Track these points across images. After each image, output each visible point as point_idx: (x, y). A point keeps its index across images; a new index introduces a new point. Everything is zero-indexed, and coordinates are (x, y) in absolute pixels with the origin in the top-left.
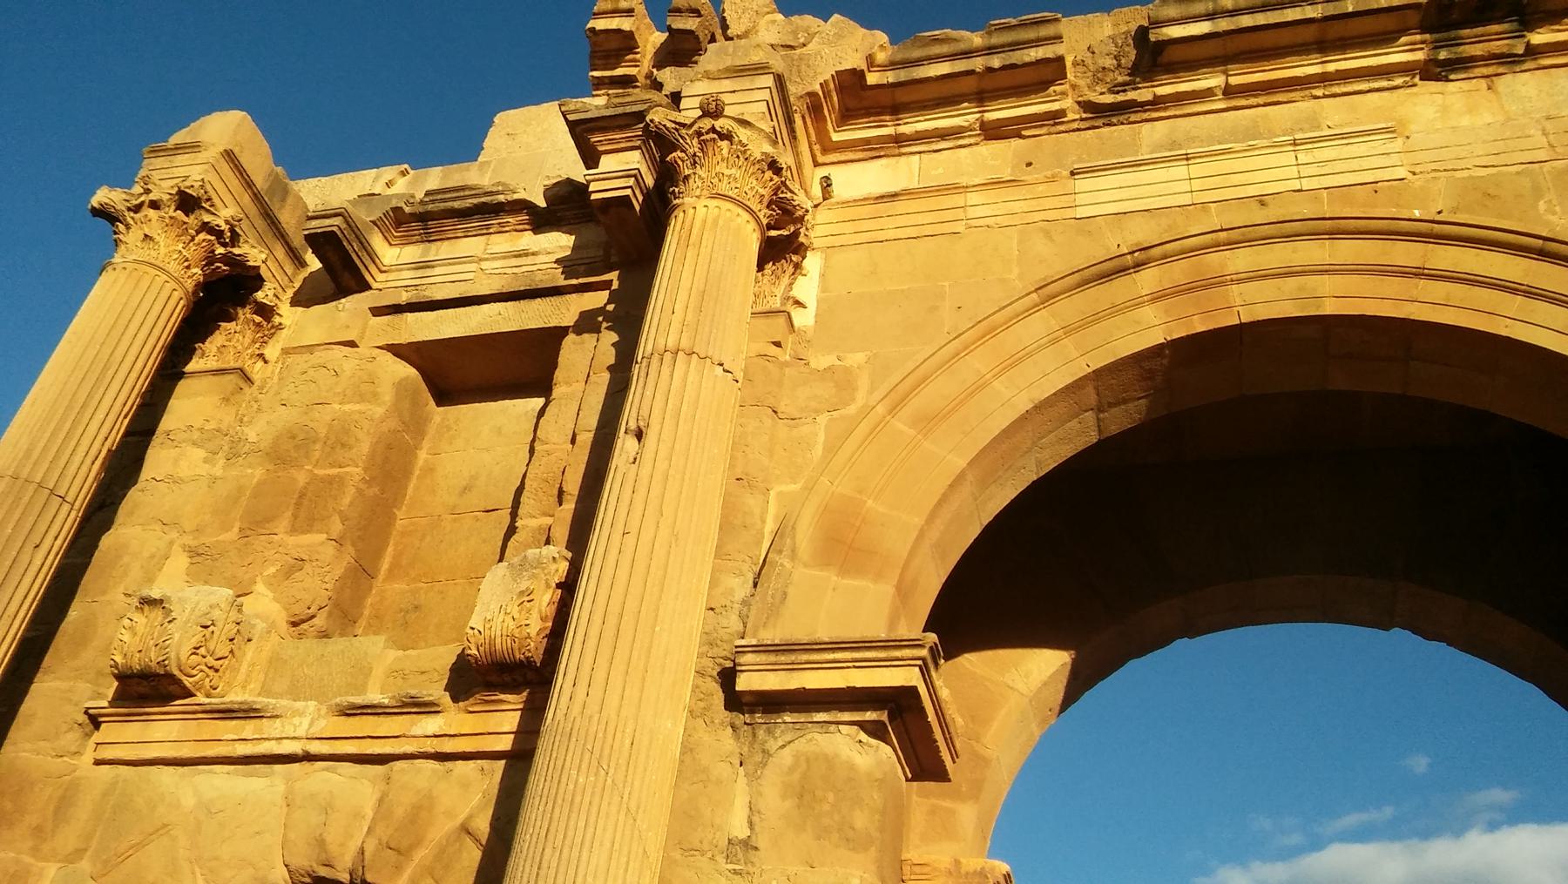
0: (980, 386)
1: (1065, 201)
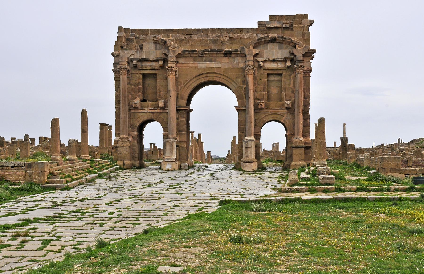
0: (191, 84)
1: (197, 66)
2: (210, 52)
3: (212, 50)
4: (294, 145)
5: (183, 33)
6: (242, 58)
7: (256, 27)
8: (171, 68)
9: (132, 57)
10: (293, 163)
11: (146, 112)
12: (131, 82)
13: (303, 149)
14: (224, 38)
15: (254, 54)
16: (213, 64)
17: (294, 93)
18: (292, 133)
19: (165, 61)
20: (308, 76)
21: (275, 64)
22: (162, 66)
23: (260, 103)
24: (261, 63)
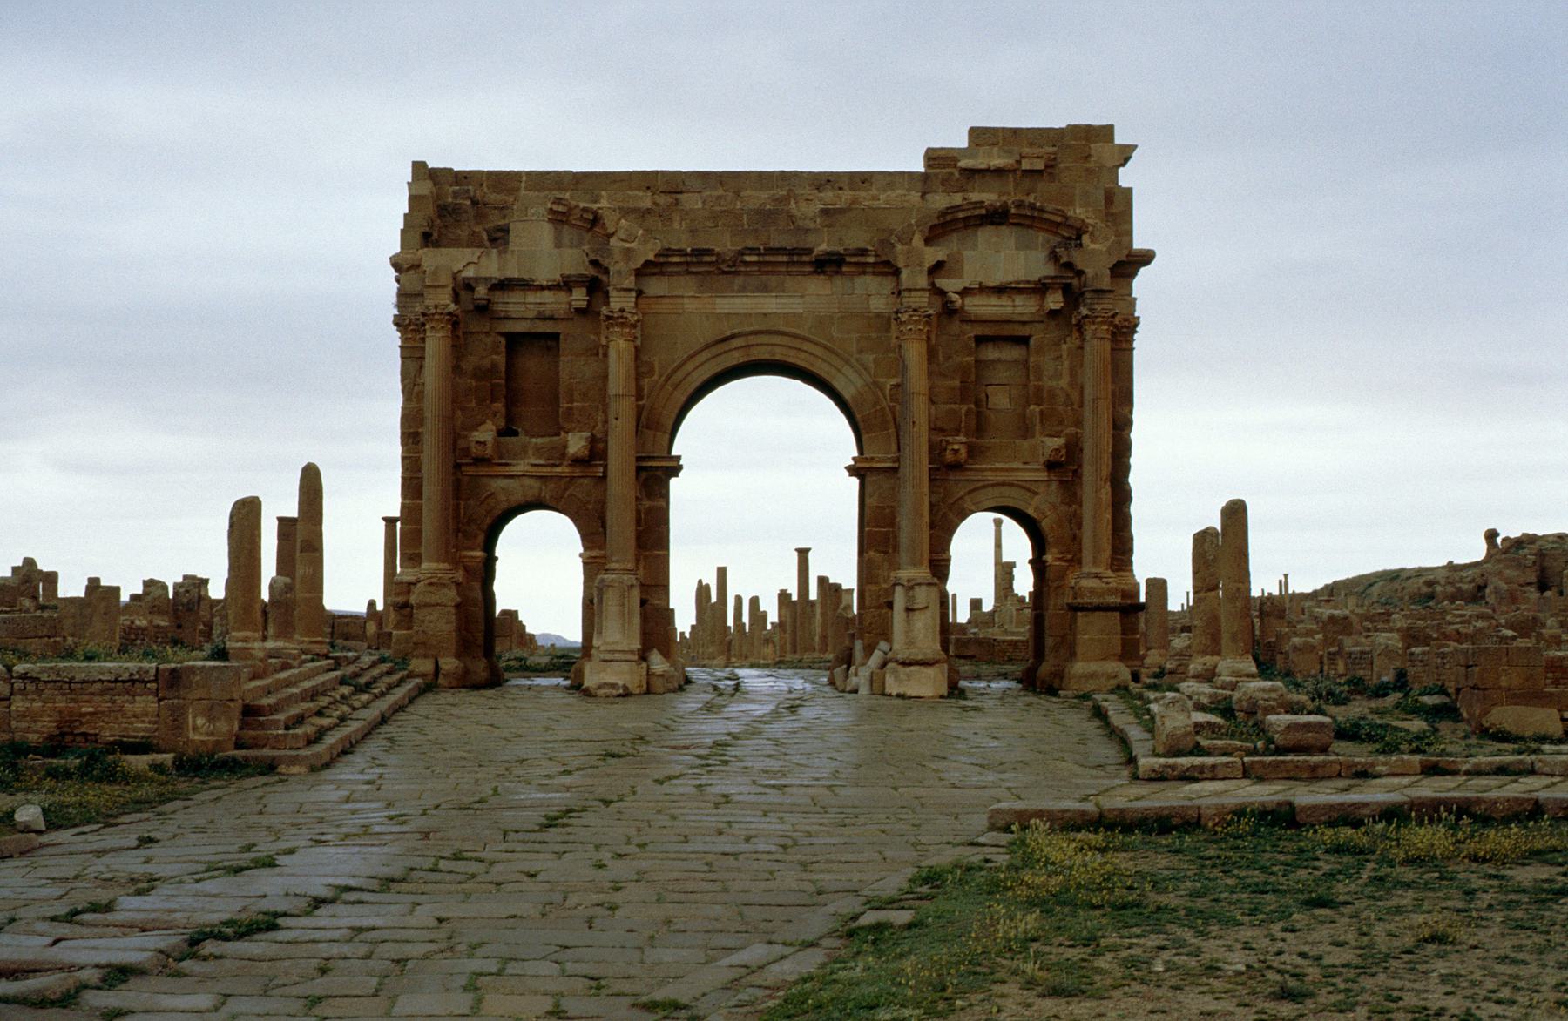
2: (764, 255)
3: (771, 249)
4: (1081, 601)
5: (648, 188)
6: (878, 279)
7: (920, 167)
8: (620, 314)
9: (470, 273)
10: (1079, 667)
11: (519, 476)
12: (464, 365)
13: (1117, 614)
14: (804, 206)
15: (927, 265)
16: (774, 301)
17: (1073, 409)
18: (1069, 557)
19: (596, 287)
20: (1124, 345)
21: (1005, 300)
22: (583, 305)
23: (953, 444)
24: (955, 297)
